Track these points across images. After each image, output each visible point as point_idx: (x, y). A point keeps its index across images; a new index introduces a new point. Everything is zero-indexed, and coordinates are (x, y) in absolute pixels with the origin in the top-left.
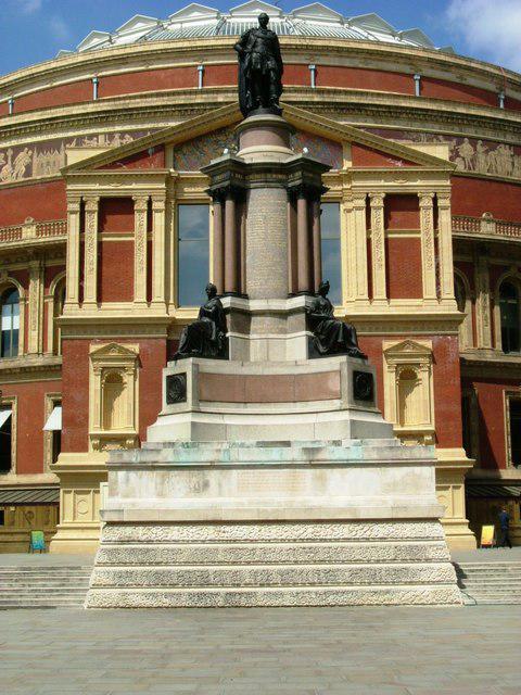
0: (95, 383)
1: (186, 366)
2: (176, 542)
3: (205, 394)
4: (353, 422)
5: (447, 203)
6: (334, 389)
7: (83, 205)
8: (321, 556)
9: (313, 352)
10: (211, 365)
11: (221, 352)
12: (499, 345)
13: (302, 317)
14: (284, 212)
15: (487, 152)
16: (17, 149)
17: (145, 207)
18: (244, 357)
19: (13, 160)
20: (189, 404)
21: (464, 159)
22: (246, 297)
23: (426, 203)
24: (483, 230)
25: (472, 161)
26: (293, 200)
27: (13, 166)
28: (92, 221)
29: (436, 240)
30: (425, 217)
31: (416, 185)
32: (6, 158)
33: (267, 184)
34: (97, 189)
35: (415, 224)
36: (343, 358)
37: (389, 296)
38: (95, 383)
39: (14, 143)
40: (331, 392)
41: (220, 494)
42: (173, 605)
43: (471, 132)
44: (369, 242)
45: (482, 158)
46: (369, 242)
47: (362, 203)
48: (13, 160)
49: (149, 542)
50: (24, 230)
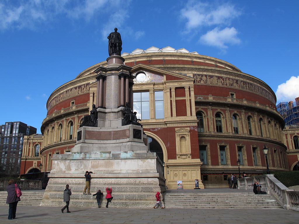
1: (82, 129)
3: (87, 137)
4: (132, 145)
5: (193, 89)
6: (127, 135)
7: (94, 94)
9: (123, 124)
10: (90, 129)
11: (95, 125)
12: (216, 130)
13: (121, 113)
15: (210, 78)
18: (104, 126)
20: (81, 141)
21: (203, 80)
22: (105, 108)
23: (187, 90)
24: (209, 99)
25: (206, 81)
26: (120, 77)
29: (190, 100)
30: (187, 93)
31: (183, 84)
32: (84, 87)
33: (112, 74)
35: (184, 95)
36: (131, 125)
37: (177, 116)
43: (205, 73)
44: (171, 101)
45: (208, 80)
46: (171, 101)
47: (169, 90)
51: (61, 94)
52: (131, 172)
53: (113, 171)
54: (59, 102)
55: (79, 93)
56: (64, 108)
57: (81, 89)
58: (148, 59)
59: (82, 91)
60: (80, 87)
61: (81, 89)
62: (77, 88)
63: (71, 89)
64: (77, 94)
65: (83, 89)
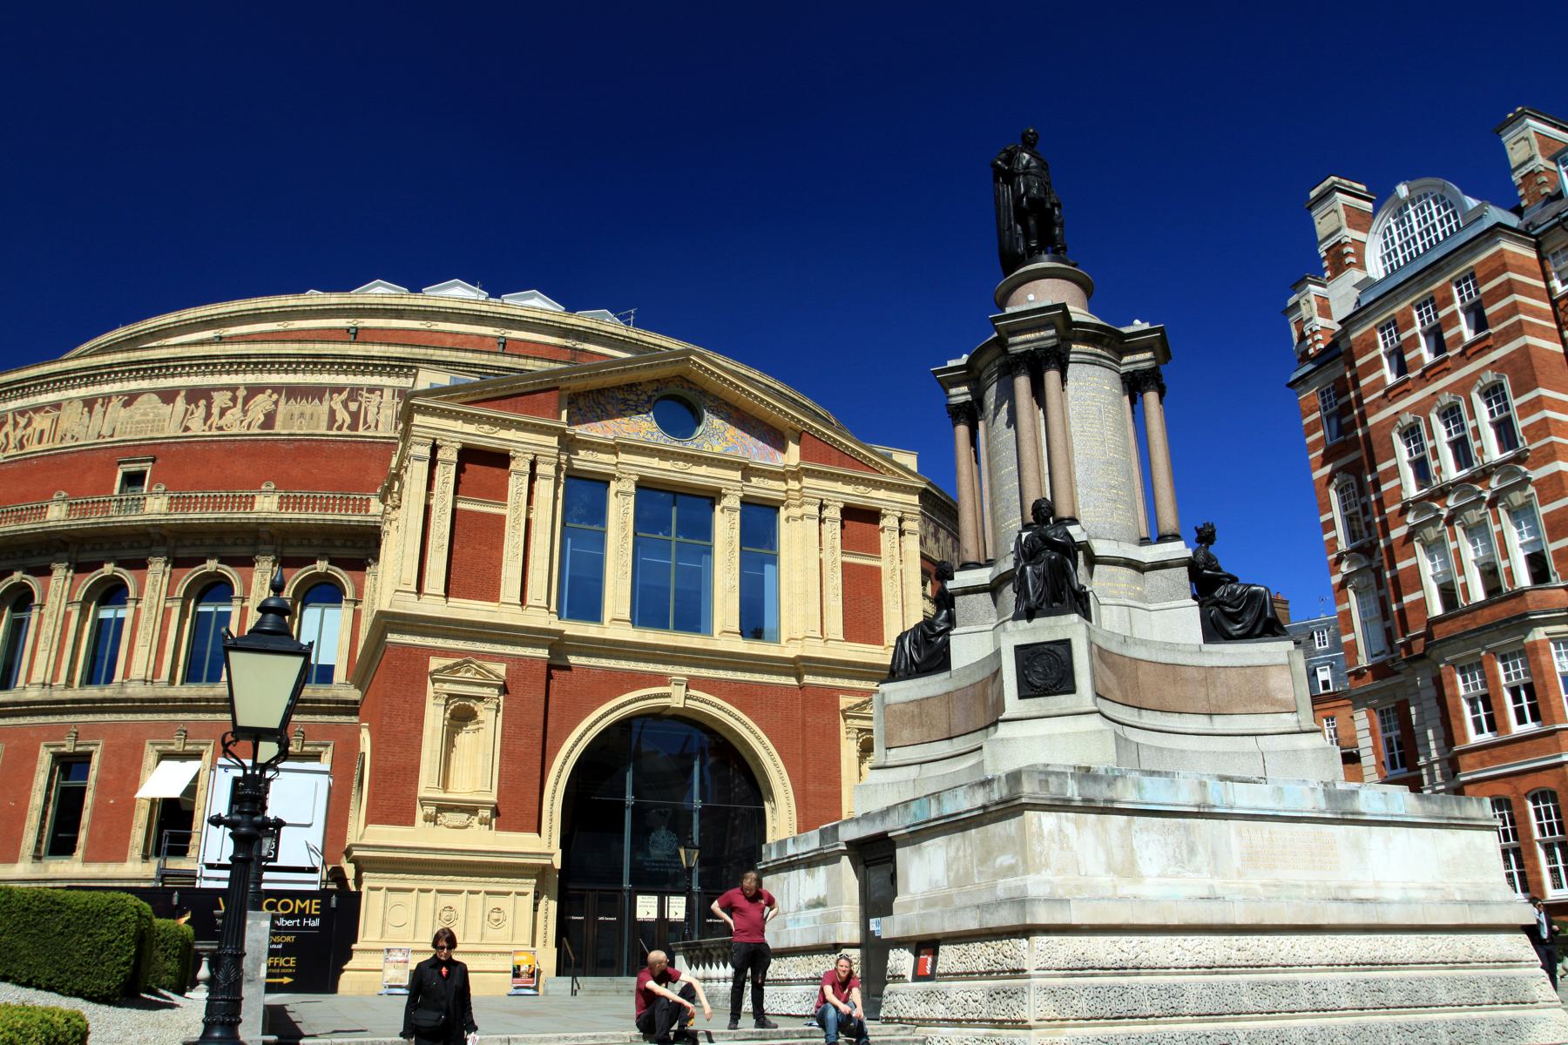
0: (435, 717)
6: (1280, 696)
7: (435, 449)
8: (1396, 998)
9: (1214, 631)
14: (1121, 404)
16: (254, 390)
17: (527, 468)
19: (246, 401)
27: (245, 412)
28: (446, 476)
31: (877, 497)
32: (234, 399)
34: (458, 432)
38: (435, 717)
39: (251, 378)
40: (1284, 703)
48: (246, 401)
49: (1120, 970)
50: (259, 499)
51: (37, 409)
52: (1421, 894)
53: (1348, 888)
54: (13, 452)
55: (187, 429)
56: (72, 494)
57: (209, 407)
58: (570, 343)
59: (215, 418)
60: (194, 395)
61: (209, 407)
62: (180, 401)
63: (131, 398)
64: (172, 430)
65: (223, 412)
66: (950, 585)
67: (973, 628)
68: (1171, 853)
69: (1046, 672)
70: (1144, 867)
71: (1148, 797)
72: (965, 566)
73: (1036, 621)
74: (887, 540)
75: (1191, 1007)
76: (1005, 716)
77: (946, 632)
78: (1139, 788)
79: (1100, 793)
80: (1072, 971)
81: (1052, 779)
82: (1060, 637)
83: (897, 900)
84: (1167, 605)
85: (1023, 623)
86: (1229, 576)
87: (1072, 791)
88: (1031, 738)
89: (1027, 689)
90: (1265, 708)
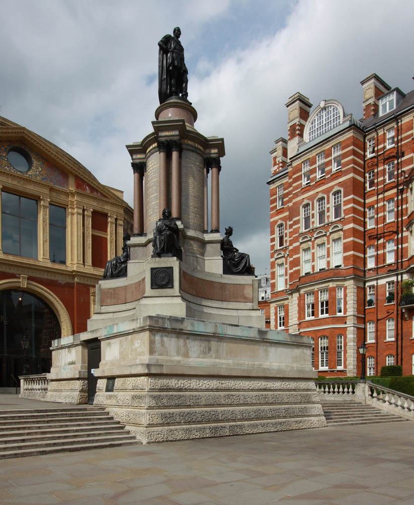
2: (196, 390)
6: (248, 296)
9: (227, 270)
31: (107, 208)
41: (217, 357)
42: (202, 436)
49: (180, 390)
66: (128, 242)
67: (136, 261)
68: (202, 350)
69: (161, 279)
70: (191, 354)
71: (196, 329)
72: (135, 235)
73: (163, 259)
74: (110, 228)
75: (203, 403)
76: (145, 295)
77: (125, 262)
78: (192, 325)
79: (178, 326)
80: (161, 390)
81: (160, 320)
82: (169, 266)
83: (101, 362)
84: (211, 258)
85: (157, 259)
86: (235, 249)
87: (167, 325)
88: (155, 305)
89: (155, 285)
90: (242, 300)
